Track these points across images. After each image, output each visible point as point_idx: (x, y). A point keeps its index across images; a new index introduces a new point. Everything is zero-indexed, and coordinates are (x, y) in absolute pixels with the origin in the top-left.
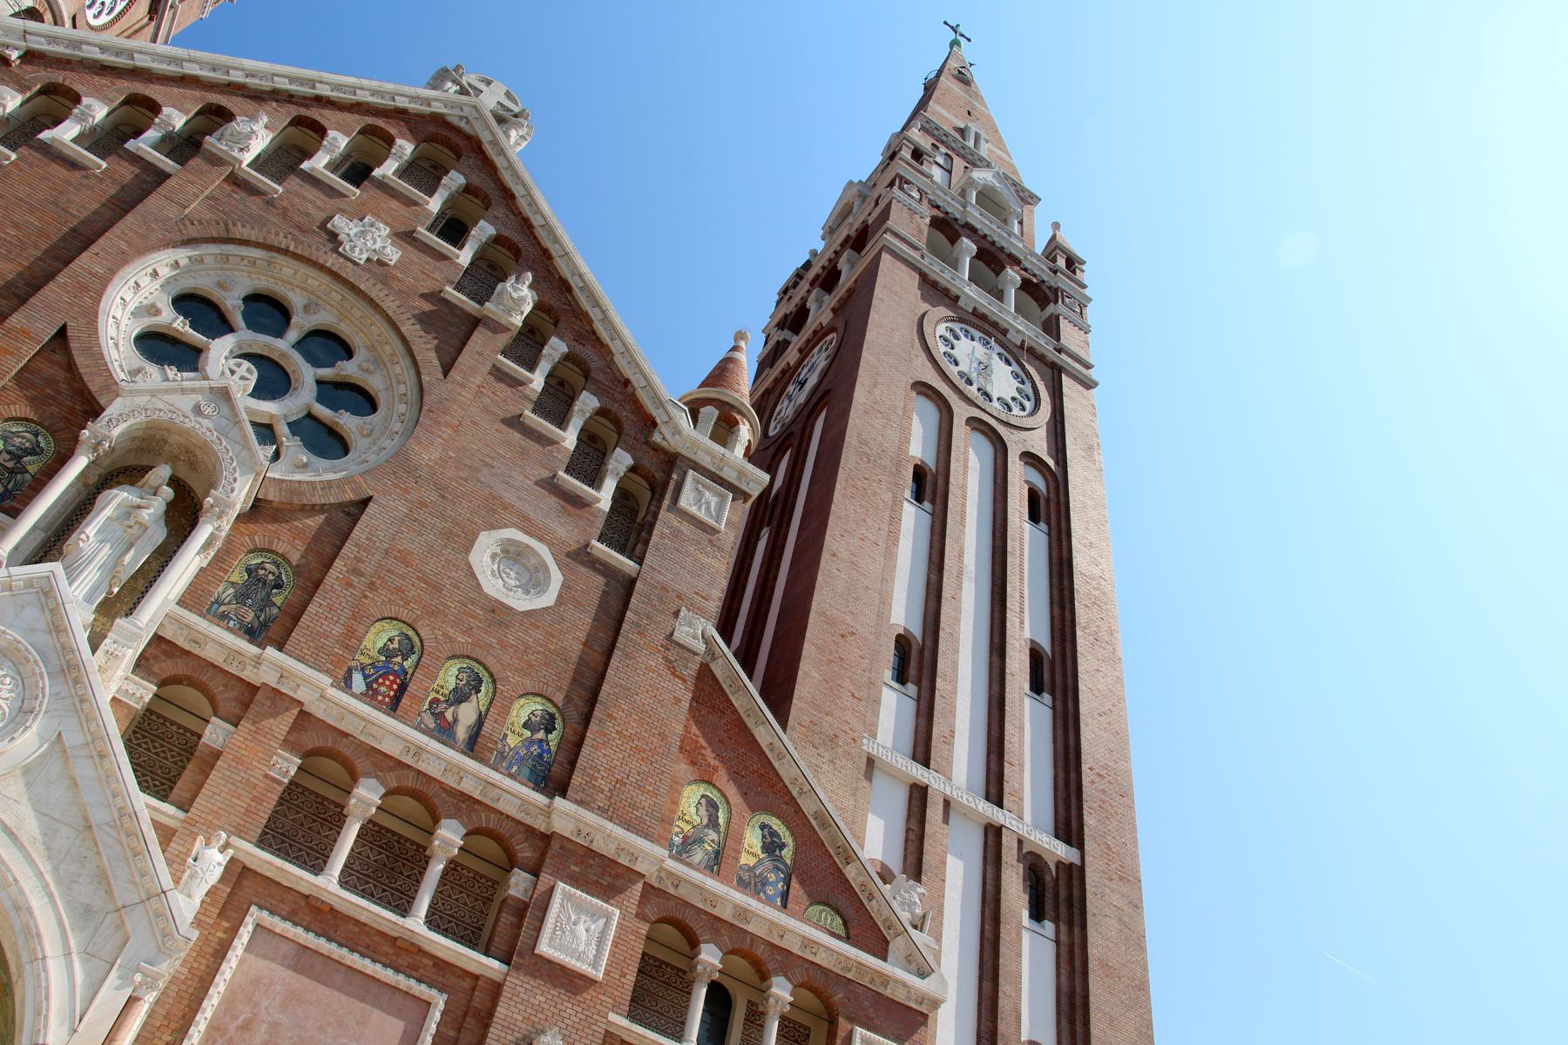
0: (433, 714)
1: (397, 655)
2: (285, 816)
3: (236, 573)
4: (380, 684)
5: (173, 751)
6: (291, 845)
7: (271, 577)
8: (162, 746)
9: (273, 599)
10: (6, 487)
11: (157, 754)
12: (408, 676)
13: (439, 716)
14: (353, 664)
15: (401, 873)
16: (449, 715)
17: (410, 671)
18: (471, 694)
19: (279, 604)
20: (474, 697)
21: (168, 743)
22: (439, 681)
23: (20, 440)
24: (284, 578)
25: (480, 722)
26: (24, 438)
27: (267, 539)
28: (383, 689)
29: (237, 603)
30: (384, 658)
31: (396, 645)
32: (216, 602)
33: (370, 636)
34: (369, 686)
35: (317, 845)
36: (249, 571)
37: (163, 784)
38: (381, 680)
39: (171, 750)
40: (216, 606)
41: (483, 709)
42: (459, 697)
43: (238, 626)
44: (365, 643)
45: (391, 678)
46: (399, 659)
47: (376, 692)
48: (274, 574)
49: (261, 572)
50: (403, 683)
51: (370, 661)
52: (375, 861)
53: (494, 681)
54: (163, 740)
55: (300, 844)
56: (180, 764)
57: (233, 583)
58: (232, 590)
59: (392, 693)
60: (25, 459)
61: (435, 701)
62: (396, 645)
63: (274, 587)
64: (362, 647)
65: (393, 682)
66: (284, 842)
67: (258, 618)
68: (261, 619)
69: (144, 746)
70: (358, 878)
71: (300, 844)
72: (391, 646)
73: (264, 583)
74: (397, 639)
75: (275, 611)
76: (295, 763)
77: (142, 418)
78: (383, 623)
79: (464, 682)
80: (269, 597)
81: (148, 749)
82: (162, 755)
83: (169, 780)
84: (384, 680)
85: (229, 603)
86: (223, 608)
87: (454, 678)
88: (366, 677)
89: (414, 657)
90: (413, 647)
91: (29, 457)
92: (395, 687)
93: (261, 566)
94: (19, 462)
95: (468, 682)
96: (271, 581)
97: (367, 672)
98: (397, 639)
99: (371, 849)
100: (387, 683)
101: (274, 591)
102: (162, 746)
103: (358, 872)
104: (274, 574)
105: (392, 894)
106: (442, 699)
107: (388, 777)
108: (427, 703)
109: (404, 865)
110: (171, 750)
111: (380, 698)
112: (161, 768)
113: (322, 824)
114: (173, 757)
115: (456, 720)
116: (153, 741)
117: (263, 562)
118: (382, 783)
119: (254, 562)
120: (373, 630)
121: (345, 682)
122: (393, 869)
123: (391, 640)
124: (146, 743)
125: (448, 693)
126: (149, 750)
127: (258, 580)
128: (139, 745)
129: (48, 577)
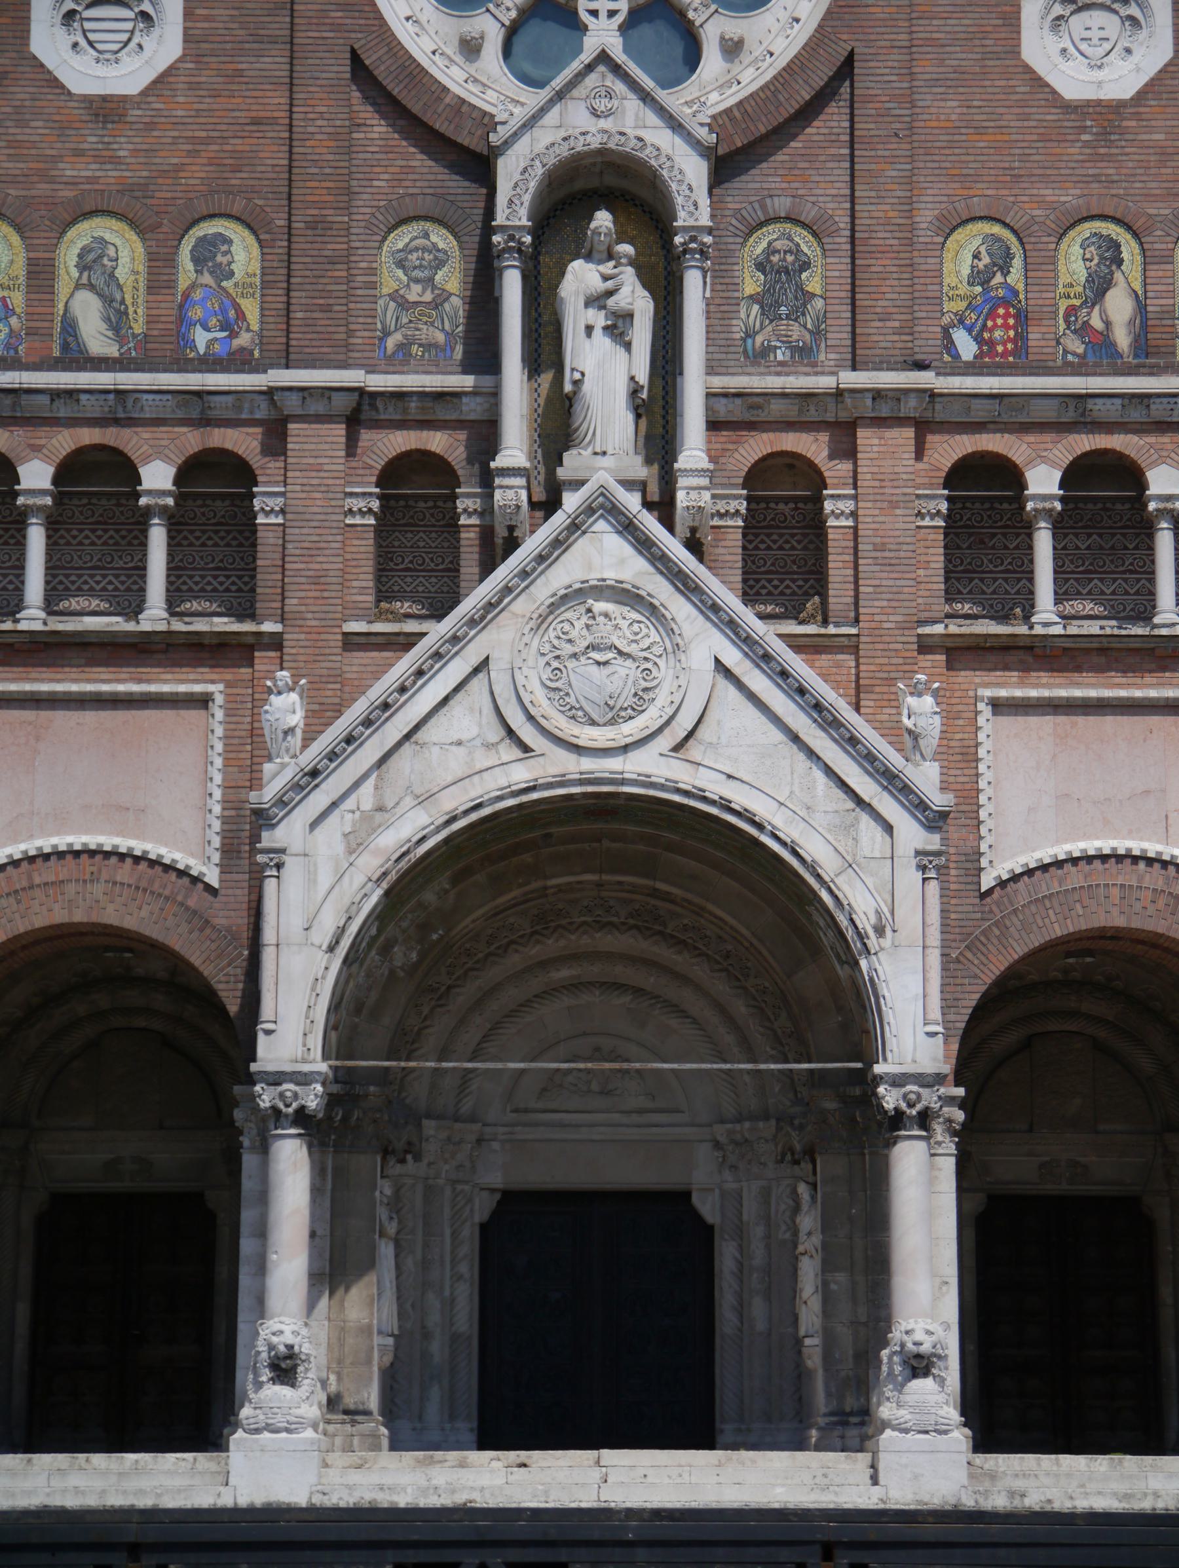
0: (1075, 332)
1: (994, 274)
2: (959, 548)
3: (748, 280)
4: (991, 330)
5: (796, 534)
6: (982, 580)
7: (790, 258)
8: (781, 535)
9: (809, 289)
10: (443, 330)
11: (781, 548)
12: (1022, 296)
13: (1084, 330)
14: (946, 320)
15: (1126, 548)
16: (1096, 323)
17: (1020, 287)
18: (1112, 273)
19: (818, 292)
20: (1118, 276)
21: (785, 528)
22: (1063, 279)
23: (415, 255)
24: (805, 250)
25: (1141, 306)
26: (417, 249)
27: (757, 206)
28: (998, 334)
29: (771, 321)
30: (979, 289)
31: (986, 260)
32: (748, 335)
33: (948, 267)
34: (979, 340)
35: (1010, 563)
36: (760, 267)
37: (806, 581)
38: (990, 324)
39: (793, 535)
40: (749, 341)
41: (1137, 286)
42: (1099, 287)
43: (788, 353)
44: (946, 281)
45: (1001, 311)
46: (998, 278)
47: (992, 343)
48: (790, 251)
49: (775, 259)
50: (1019, 310)
51: (965, 304)
52: (1088, 548)
53: (1136, 235)
54: (778, 527)
55: (991, 572)
56: (811, 546)
57: (751, 297)
58: (756, 307)
59: (1012, 333)
60: (437, 278)
61: (1071, 311)
62: (986, 260)
63: (801, 271)
64: (945, 289)
65: (1007, 316)
66: (971, 580)
67: (805, 326)
68: (809, 326)
69: (762, 546)
70: (1076, 580)
71: (991, 572)
72: (981, 265)
73: (787, 273)
74: (983, 249)
75: (819, 303)
76: (943, 495)
77: (539, 171)
78: (955, 236)
79: (1096, 261)
80: (802, 290)
81: (769, 548)
82: (787, 546)
83: (811, 572)
84: (994, 320)
85: (762, 329)
86: (759, 339)
87: (1082, 262)
88: (969, 330)
89: (1017, 263)
90: (1009, 248)
91: (440, 273)
92: (1011, 321)
93: (770, 250)
94: (434, 287)
95: (1102, 258)
96: (793, 264)
97: (968, 322)
98: (983, 249)
99: (1076, 535)
100: (999, 321)
101: (804, 275)
102: (781, 535)
103: (1073, 572)
104: (790, 251)
105: (1125, 580)
106: (1077, 302)
107: (1057, 452)
108: (1061, 321)
109: (1124, 535)
110: (793, 535)
111: (1000, 349)
112: (794, 562)
113: (1004, 535)
114: (799, 542)
115: (1108, 324)
116: (768, 535)
117: (770, 244)
118: (1053, 465)
119: (759, 250)
120: (948, 255)
121: (949, 353)
122: (1112, 548)
123: (976, 256)
124: (763, 542)
125: (1080, 289)
126: (771, 549)
127: (778, 272)
128: (756, 548)
129: (602, 494)
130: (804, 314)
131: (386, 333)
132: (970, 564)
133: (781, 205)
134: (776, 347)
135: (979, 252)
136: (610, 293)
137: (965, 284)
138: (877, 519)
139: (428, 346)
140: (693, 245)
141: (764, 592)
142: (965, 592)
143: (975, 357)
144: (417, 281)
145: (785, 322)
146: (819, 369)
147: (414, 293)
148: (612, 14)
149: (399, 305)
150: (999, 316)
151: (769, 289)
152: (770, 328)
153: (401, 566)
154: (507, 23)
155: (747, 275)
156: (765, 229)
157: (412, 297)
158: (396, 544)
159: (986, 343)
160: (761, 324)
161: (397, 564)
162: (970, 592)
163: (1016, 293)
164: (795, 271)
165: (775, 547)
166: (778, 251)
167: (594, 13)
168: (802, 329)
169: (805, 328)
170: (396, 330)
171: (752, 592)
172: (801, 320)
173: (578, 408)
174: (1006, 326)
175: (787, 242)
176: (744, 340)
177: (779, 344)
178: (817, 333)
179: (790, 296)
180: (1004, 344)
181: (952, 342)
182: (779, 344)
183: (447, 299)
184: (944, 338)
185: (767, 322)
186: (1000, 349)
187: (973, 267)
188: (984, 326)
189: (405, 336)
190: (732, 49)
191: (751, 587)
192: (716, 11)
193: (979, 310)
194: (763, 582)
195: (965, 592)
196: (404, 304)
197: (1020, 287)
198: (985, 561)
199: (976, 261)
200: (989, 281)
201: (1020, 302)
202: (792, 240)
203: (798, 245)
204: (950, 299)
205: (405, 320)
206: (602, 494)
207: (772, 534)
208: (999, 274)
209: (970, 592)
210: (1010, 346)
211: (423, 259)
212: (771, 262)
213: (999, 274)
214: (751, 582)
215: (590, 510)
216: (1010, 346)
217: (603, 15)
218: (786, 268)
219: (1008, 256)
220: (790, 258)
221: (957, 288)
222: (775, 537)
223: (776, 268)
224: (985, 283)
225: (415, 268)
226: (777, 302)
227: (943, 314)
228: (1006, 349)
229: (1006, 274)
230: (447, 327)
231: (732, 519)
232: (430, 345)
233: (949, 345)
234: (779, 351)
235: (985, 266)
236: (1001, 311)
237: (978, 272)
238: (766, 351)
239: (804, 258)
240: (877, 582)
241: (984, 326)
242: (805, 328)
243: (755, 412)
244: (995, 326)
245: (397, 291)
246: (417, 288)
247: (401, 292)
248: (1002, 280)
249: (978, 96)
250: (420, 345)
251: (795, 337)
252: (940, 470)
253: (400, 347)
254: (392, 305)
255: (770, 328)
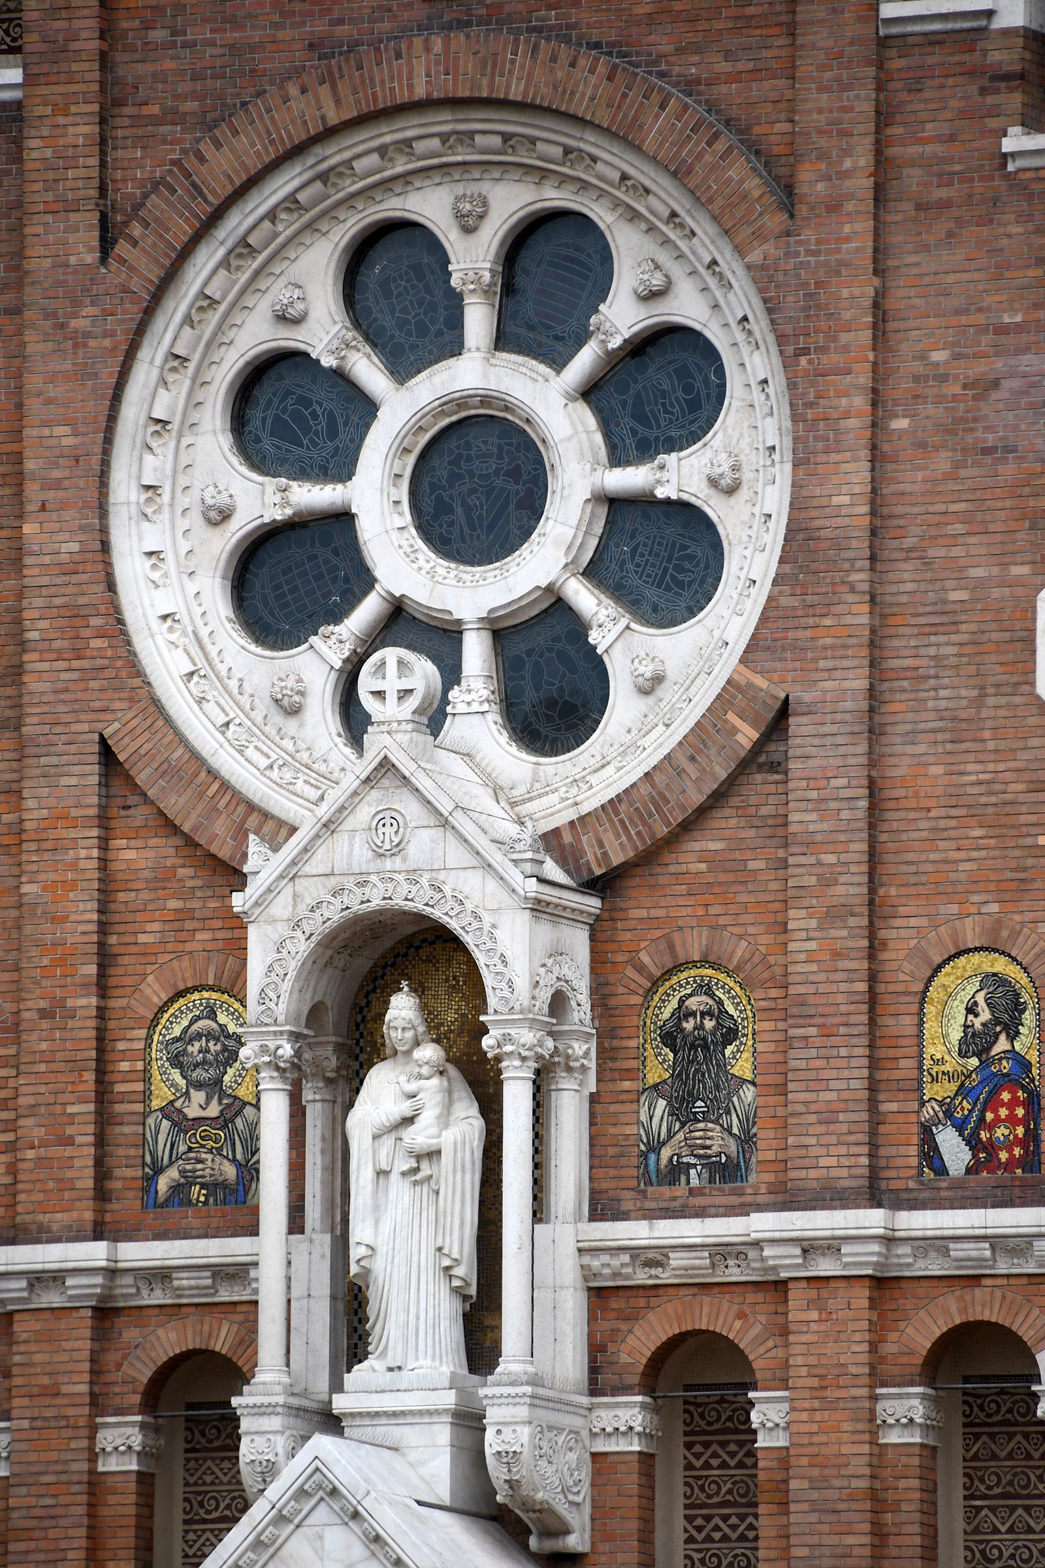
2: (995, 1457)
3: (651, 1061)
4: (991, 1127)
7: (709, 1024)
9: (734, 1071)
12: (1035, 1071)
14: (928, 1112)
19: (748, 1076)
24: (731, 1009)
29: (683, 1125)
30: (974, 1061)
31: (985, 1015)
34: (973, 1143)
38: (989, 1116)
40: (652, 1157)
43: (706, 1175)
44: (929, 1050)
45: (1006, 1096)
46: (1002, 1044)
47: (991, 1148)
48: (708, 1013)
49: (689, 1025)
51: (953, 1087)
57: (655, 1086)
58: (662, 1103)
59: (1020, 1131)
62: (985, 1015)
63: (727, 1042)
64: (927, 1063)
65: (1013, 1104)
67: (729, 1130)
68: (735, 1131)
69: (715, 1462)
72: (978, 1023)
73: (705, 1047)
75: (748, 1093)
80: (727, 1072)
85: (670, 1135)
86: (666, 1153)
88: (960, 1128)
92: (1020, 1112)
93: (682, 1013)
96: (713, 1034)
98: (980, 998)
100: (1003, 1112)
101: (728, 1051)
111: (1003, 1156)
116: (724, 1445)
117: (681, 1001)
119: (666, 1014)
123: (971, 1010)
124: (715, 1455)
128: (707, 1466)
129: (317, 1469)
130: (728, 1113)
131: (158, 1170)
132: (1011, 1483)
133: (694, 945)
134: (689, 1166)
135: (976, 1004)
136: (409, 1121)
137: (955, 1055)
138: (815, 1439)
139: (214, 1187)
140: (508, 1048)
141: (717, 1536)
142: (1003, 1529)
143: (969, 1171)
144: (199, 1086)
145: (701, 1125)
146: (749, 1199)
147: (196, 1106)
148: (405, 694)
149: (175, 1124)
150: (1003, 1104)
151: (680, 1074)
152: (680, 1136)
153: (215, 1515)
154: (338, 664)
155: (650, 1052)
156: (674, 980)
157: (193, 1112)
158: (208, 1479)
159: (984, 1149)
160: (669, 1131)
161: (208, 1512)
162: (1011, 1530)
163: (1026, 1066)
164: (715, 1044)
165: (732, 1463)
166: (693, 1014)
167: (380, 694)
168: (726, 1135)
169: (730, 1133)
170: (171, 1163)
171: (699, 1537)
172: (724, 1120)
173: (372, 1294)
174: (1012, 1120)
175: (704, 998)
176: (644, 1155)
177: (693, 1161)
178: (747, 1140)
179: (709, 1083)
180: (1010, 1151)
181: (936, 1148)
182: (693, 1161)
183: (239, 1112)
184: (923, 1142)
185: (678, 1125)
186: (1003, 1156)
187: (966, 1026)
188: (982, 1119)
189: (183, 1173)
190: (650, 686)
191: (699, 1529)
192: (628, 627)
193: (974, 1093)
194: (717, 1521)
195: (1003, 1529)
196: (181, 1124)
197: (1033, 1056)
198: (1033, 1478)
199: (971, 1017)
200: (990, 1049)
201: (1033, 1080)
202: (712, 995)
203: (720, 1003)
204: (935, 1079)
205: (183, 1148)
206: (317, 1469)
207: (728, 1442)
208: (1003, 1037)
209: (1011, 1530)
210: (1017, 1151)
211: (208, 1051)
212: (683, 1030)
213: (1003, 1037)
214: (699, 1522)
215: (302, 1494)
216: (1017, 1151)
217: (392, 697)
218: (704, 1039)
219: (1018, 1008)
220: (709, 1024)
221: (942, 1061)
222: (732, 1447)
223: (690, 1039)
224: (982, 1052)
225: (197, 1065)
226: (690, 1094)
227: (923, 1104)
228: (1012, 1155)
229: (1013, 1036)
230: (239, 1156)
231: (622, 1440)
232: (216, 1185)
233: (931, 1155)
234: (693, 1172)
235: (983, 1025)
236: (1006, 1096)
237: (974, 1035)
238: (676, 1171)
239: (729, 1024)
240: (815, 1540)
241: (982, 1119)
242: (730, 1133)
243: (653, 1272)
244: (997, 1120)
245: (172, 1102)
246: (198, 1097)
247: (178, 1104)
248: (1009, 1047)
249: (972, 757)
250: (203, 1186)
251: (715, 1149)
252: (912, 1353)
253: (176, 1189)
254: (166, 1124)
255: (680, 1136)
